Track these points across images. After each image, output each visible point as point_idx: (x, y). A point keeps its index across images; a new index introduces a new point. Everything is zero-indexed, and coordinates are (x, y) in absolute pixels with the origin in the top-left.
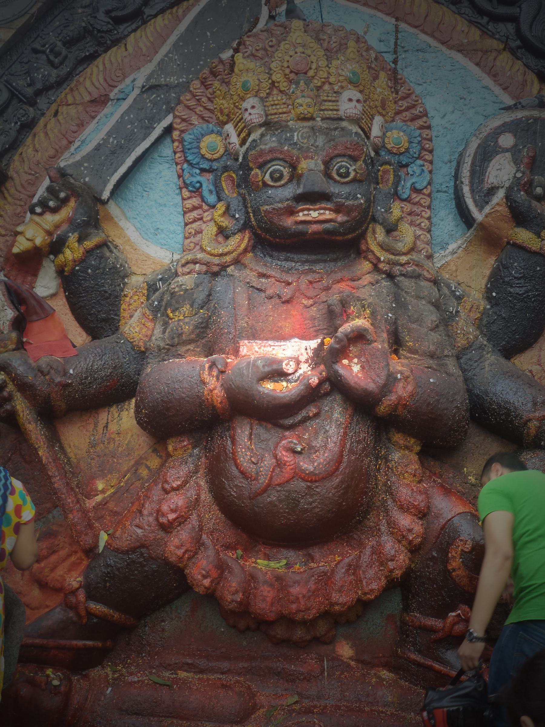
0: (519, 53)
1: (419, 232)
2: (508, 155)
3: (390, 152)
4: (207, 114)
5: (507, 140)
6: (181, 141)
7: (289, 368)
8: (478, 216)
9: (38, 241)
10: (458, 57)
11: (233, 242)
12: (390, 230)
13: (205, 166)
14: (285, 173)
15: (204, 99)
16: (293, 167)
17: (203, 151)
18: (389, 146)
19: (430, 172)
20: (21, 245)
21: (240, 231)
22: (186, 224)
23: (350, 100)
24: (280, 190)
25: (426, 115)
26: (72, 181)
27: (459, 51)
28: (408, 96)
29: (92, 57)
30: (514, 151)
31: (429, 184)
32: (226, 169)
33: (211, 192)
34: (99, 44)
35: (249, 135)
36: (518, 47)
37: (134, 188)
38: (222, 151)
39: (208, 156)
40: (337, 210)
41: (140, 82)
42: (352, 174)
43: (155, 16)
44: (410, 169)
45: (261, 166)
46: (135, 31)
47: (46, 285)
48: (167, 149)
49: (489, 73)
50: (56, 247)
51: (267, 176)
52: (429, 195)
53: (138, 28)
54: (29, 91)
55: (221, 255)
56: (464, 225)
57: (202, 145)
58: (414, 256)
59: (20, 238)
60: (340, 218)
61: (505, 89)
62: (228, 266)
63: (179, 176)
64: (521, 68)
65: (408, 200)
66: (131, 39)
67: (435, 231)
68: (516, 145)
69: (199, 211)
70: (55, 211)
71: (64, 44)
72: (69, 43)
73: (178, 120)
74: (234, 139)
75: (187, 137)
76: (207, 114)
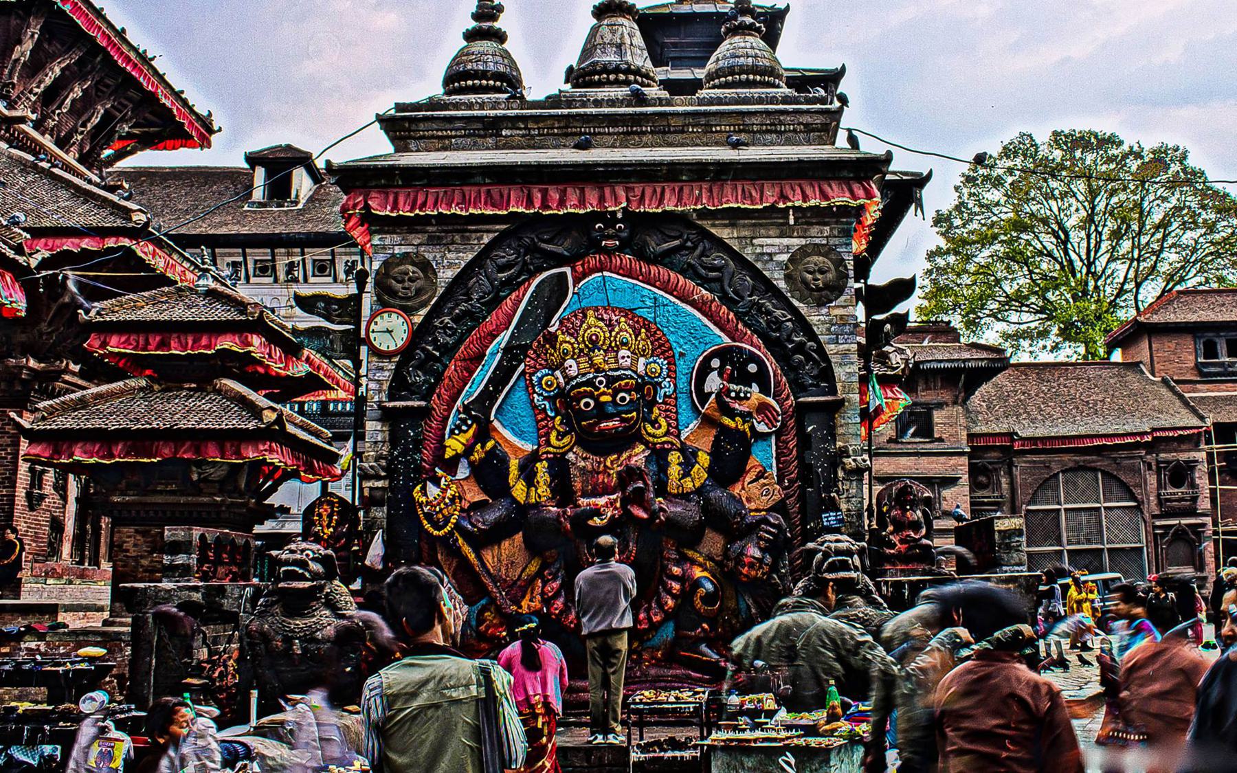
5: (716, 363)
11: (566, 440)
12: (654, 423)
13: (545, 394)
20: (449, 454)
22: (539, 429)
25: (671, 348)
29: (473, 328)
31: (675, 391)
37: (507, 407)
40: (623, 420)
47: (463, 472)
55: (559, 448)
61: (716, 324)
70: (465, 432)
74: (561, 380)
75: (534, 378)
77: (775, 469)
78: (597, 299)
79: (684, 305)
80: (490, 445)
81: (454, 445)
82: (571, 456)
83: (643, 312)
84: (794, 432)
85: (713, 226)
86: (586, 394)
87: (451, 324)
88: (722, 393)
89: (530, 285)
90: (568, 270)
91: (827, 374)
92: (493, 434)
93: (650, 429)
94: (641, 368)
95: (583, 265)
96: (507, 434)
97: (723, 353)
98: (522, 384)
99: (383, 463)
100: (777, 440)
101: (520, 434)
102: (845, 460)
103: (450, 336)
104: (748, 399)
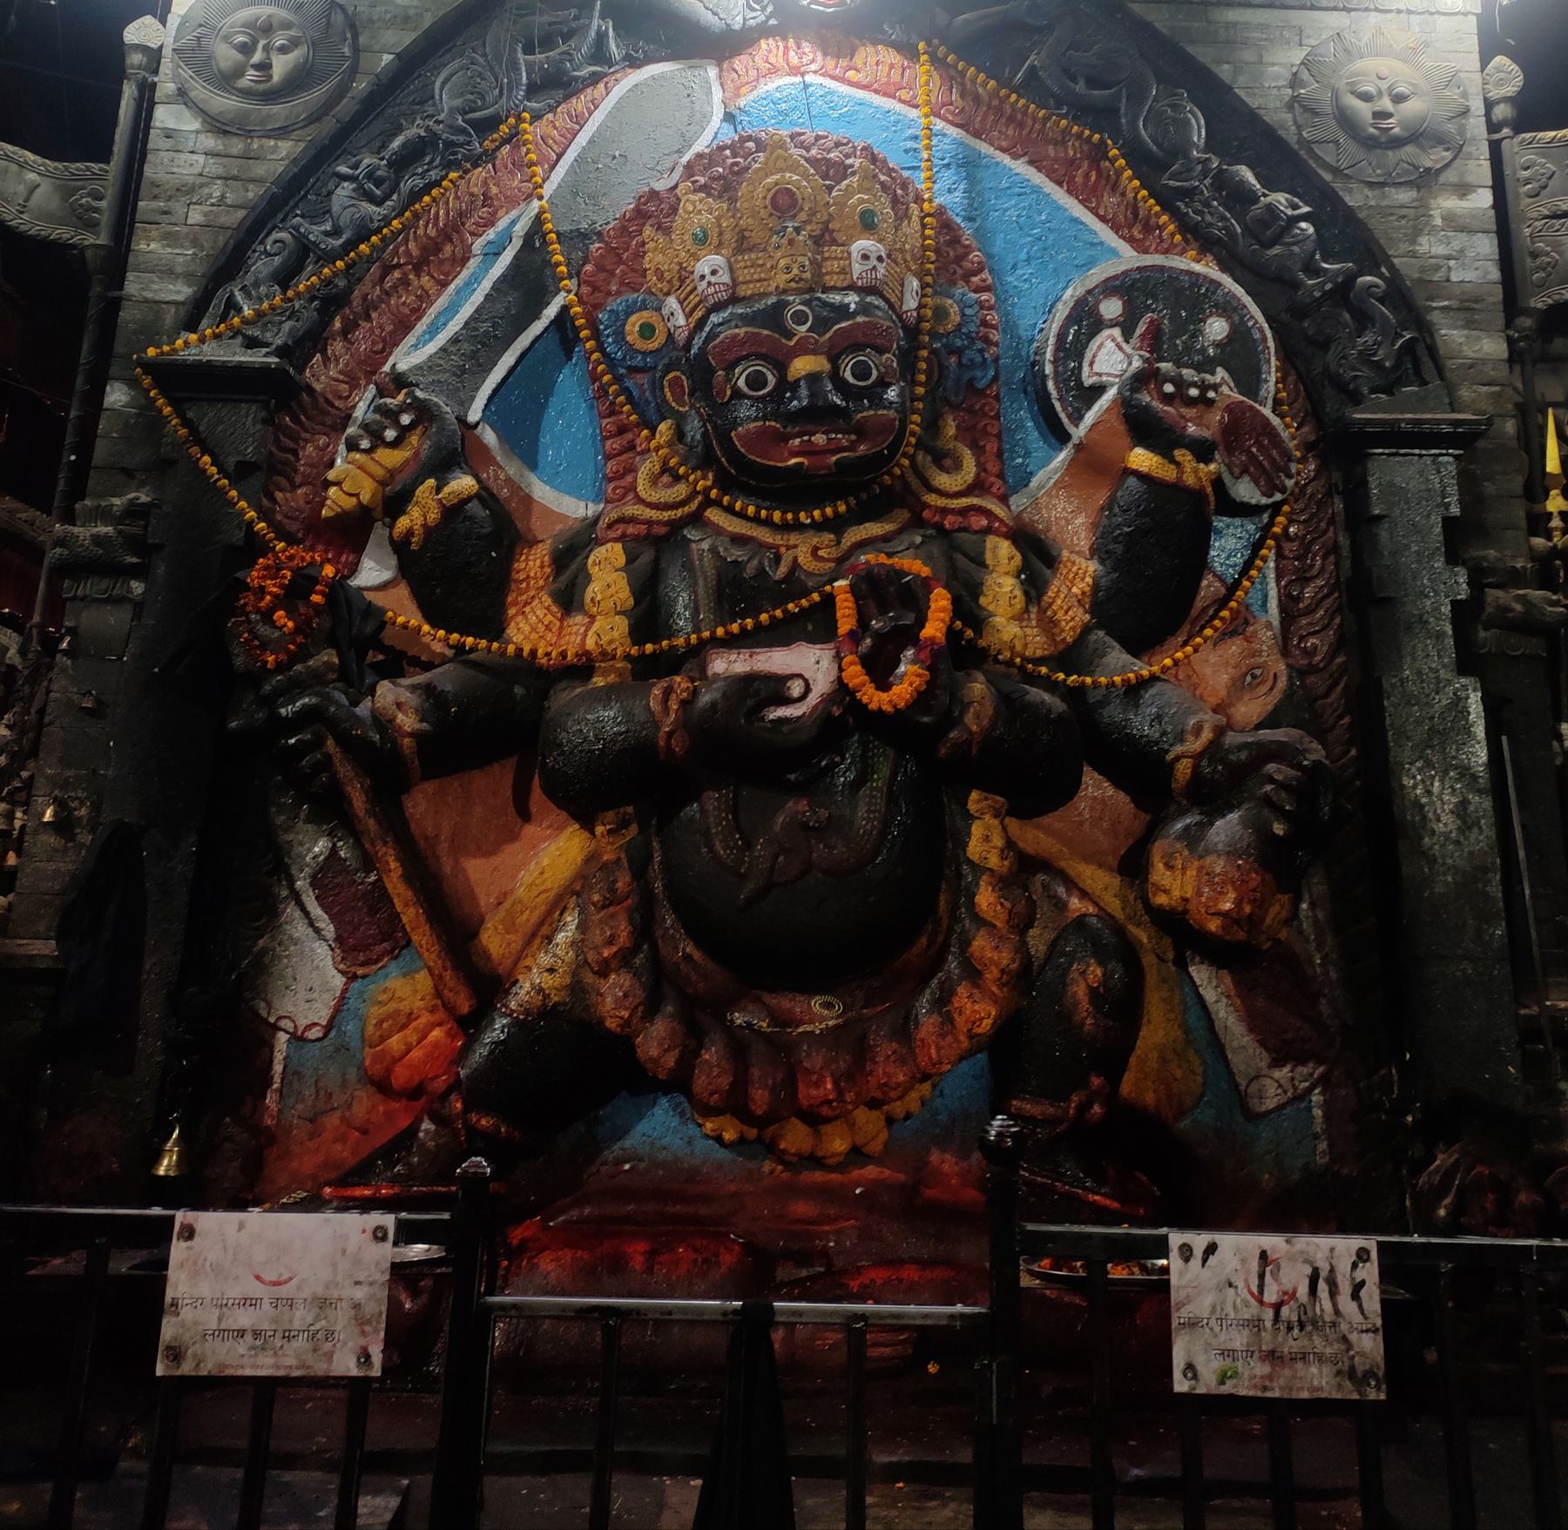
8: (1079, 432)
26: (419, 394)
31: (995, 378)
50: (396, 501)
51: (741, 383)
62: (683, 527)
70: (395, 444)
74: (681, 321)
82: (691, 534)
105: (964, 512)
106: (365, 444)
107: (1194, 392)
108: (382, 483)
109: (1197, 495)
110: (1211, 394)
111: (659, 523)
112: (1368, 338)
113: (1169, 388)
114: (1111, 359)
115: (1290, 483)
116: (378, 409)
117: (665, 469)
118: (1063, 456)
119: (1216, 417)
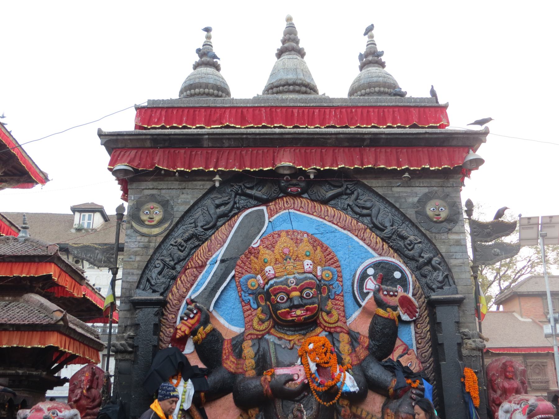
0: (373, 229)
1: (340, 312)
2: (372, 277)
3: (324, 280)
4: (248, 270)
5: (371, 271)
6: (239, 282)
7: (296, 378)
8: (363, 304)
9: (187, 332)
10: (349, 233)
12: (329, 313)
14: (285, 298)
15: (247, 263)
16: (288, 295)
17: (250, 286)
18: (324, 278)
19: (342, 286)
20: (179, 334)
21: (268, 319)
22: (245, 318)
23: (308, 265)
24: (283, 305)
26: (198, 305)
27: (349, 231)
28: (330, 254)
30: (374, 276)
31: (342, 291)
32: (259, 293)
33: (254, 303)
34: (200, 241)
35: (269, 280)
36: (373, 227)
38: (257, 286)
39: (252, 288)
40: (307, 310)
41: (219, 258)
42: (311, 295)
43: (222, 226)
44: (334, 286)
45: (275, 295)
46: (213, 233)
47: (189, 349)
48: (233, 285)
49: (362, 239)
52: (343, 296)
53: (215, 232)
54: (172, 263)
56: (357, 306)
57: (248, 283)
58: (339, 324)
59: (179, 331)
60: (308, 313)
61: (369, 246)
63: (240, 297)
64: (375, 236)
65: (334, 299)
66: (213, 237)
67: (347, 311)
68: (375, 273)
69: (250, 312)
71: (185, 241)
72: (186, 241)
73: (237, 273)
74: (262, 282)
76: (248, 270)
77: (415, 348)
78: (286, 226)
79: (346, 232)
80: (209, 328)
81: (183, 328)
82: (267, 337)
83: (318, 237)
84: (428, 320)
85: (366, 178)
86: (280, 291)
87: (183, 243)
88: (377, 292)
89: (238, 217)
90: (264, 208)
91: (448, 279)
92: (211, 320)
93: (326, 318)
94: (319, 273)
95: (275, 205)
96: (222, 321)
97: (376, 266)
98: (233, 285)
99: (130, 342)
100: (416, 326)
101: (231, 321)
102: (466, 341)
103: (182, 251)
104: (396, 296)
105: (334, 328)
106: (185, 318)
107: (391, 293)
108: (190, 328)
109: (394, 320)
110: (396, 294)
111: (260, 335)
112: (435, 274)
113: (385, 293)
114: (371, 285)
115: (417, 315)
116: (188, 309)
117: (260, 320)
118: (360, 310)
119: (397, 299)
